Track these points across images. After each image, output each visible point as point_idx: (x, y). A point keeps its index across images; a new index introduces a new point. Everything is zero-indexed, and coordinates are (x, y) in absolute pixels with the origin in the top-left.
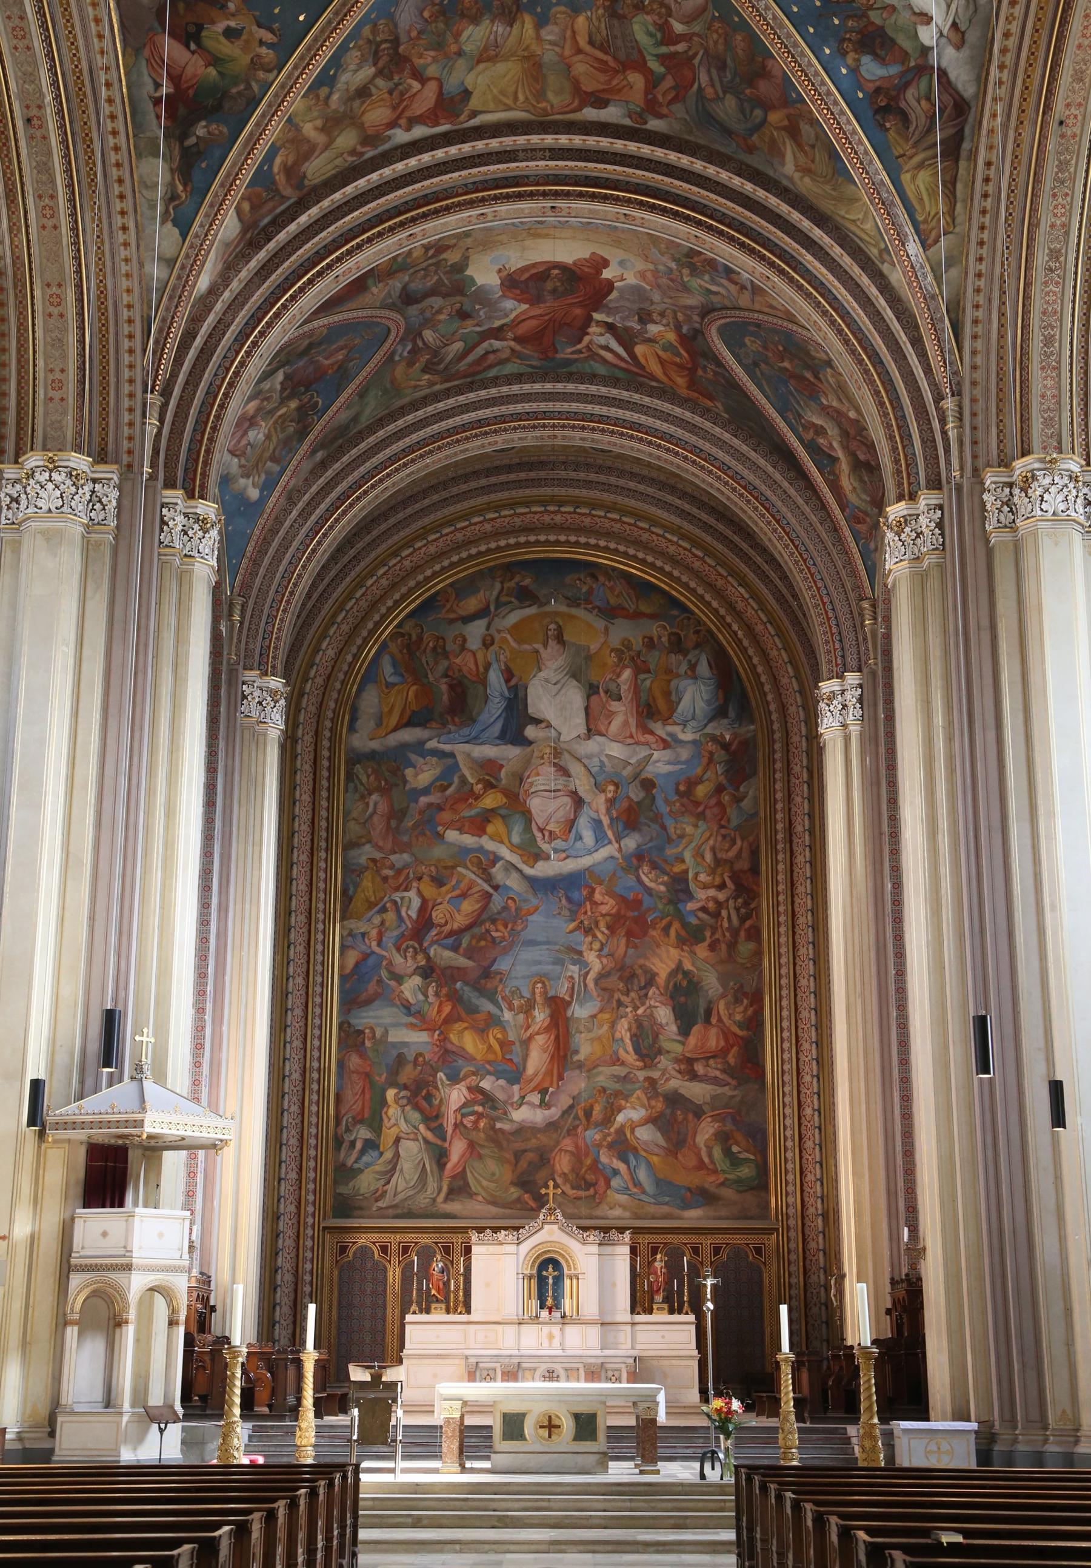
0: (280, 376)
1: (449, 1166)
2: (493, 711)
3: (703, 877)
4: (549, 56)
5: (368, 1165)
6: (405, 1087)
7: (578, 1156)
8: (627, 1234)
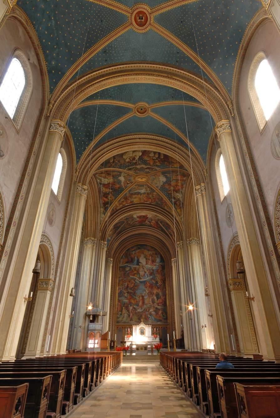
1: (130, 317)
2: (136, 262)
3: (159, 281)
7: (145, 315)
8: (151, 325)
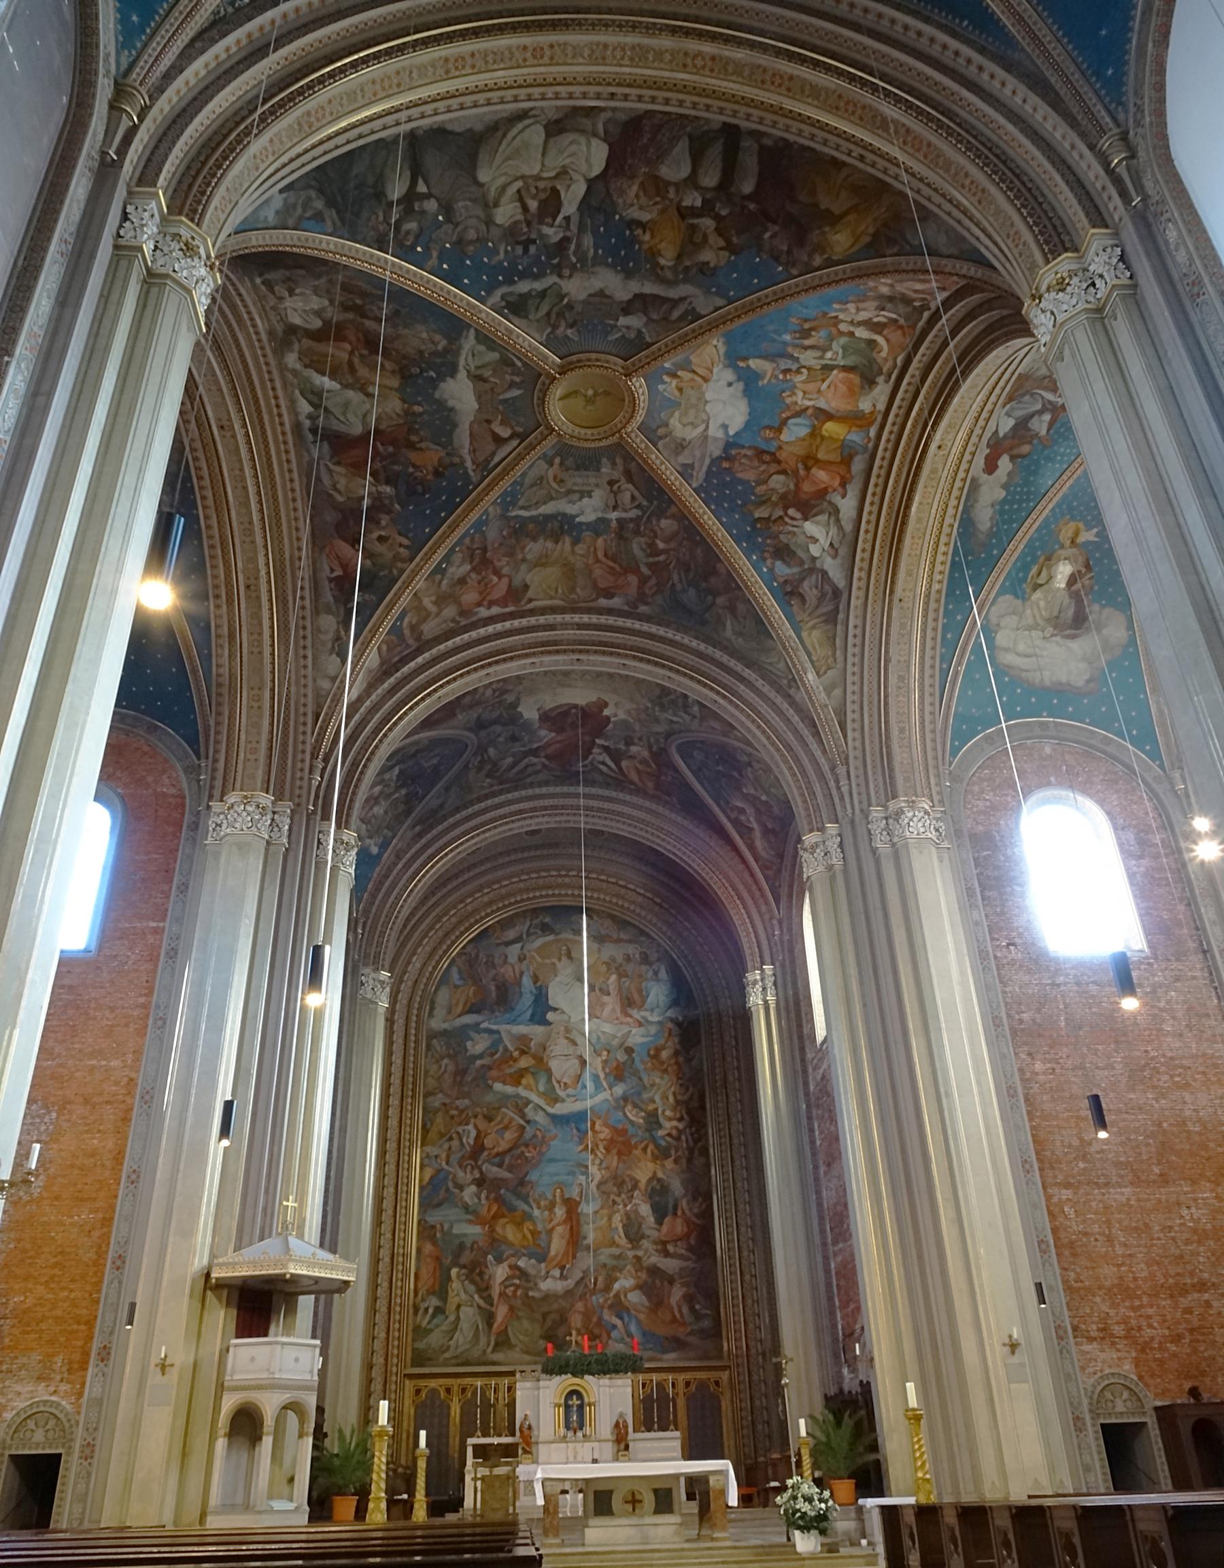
0: (396, 771)
2: (526, 1001)
3: (668, 1113)
4: (579, 565)
5: (437, 1326)
6: (464, 1267)
7: (587, 1315)
